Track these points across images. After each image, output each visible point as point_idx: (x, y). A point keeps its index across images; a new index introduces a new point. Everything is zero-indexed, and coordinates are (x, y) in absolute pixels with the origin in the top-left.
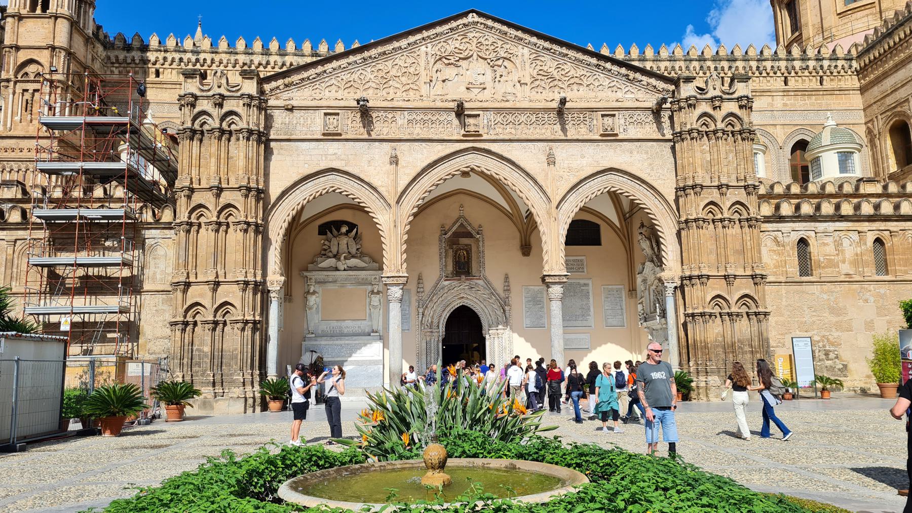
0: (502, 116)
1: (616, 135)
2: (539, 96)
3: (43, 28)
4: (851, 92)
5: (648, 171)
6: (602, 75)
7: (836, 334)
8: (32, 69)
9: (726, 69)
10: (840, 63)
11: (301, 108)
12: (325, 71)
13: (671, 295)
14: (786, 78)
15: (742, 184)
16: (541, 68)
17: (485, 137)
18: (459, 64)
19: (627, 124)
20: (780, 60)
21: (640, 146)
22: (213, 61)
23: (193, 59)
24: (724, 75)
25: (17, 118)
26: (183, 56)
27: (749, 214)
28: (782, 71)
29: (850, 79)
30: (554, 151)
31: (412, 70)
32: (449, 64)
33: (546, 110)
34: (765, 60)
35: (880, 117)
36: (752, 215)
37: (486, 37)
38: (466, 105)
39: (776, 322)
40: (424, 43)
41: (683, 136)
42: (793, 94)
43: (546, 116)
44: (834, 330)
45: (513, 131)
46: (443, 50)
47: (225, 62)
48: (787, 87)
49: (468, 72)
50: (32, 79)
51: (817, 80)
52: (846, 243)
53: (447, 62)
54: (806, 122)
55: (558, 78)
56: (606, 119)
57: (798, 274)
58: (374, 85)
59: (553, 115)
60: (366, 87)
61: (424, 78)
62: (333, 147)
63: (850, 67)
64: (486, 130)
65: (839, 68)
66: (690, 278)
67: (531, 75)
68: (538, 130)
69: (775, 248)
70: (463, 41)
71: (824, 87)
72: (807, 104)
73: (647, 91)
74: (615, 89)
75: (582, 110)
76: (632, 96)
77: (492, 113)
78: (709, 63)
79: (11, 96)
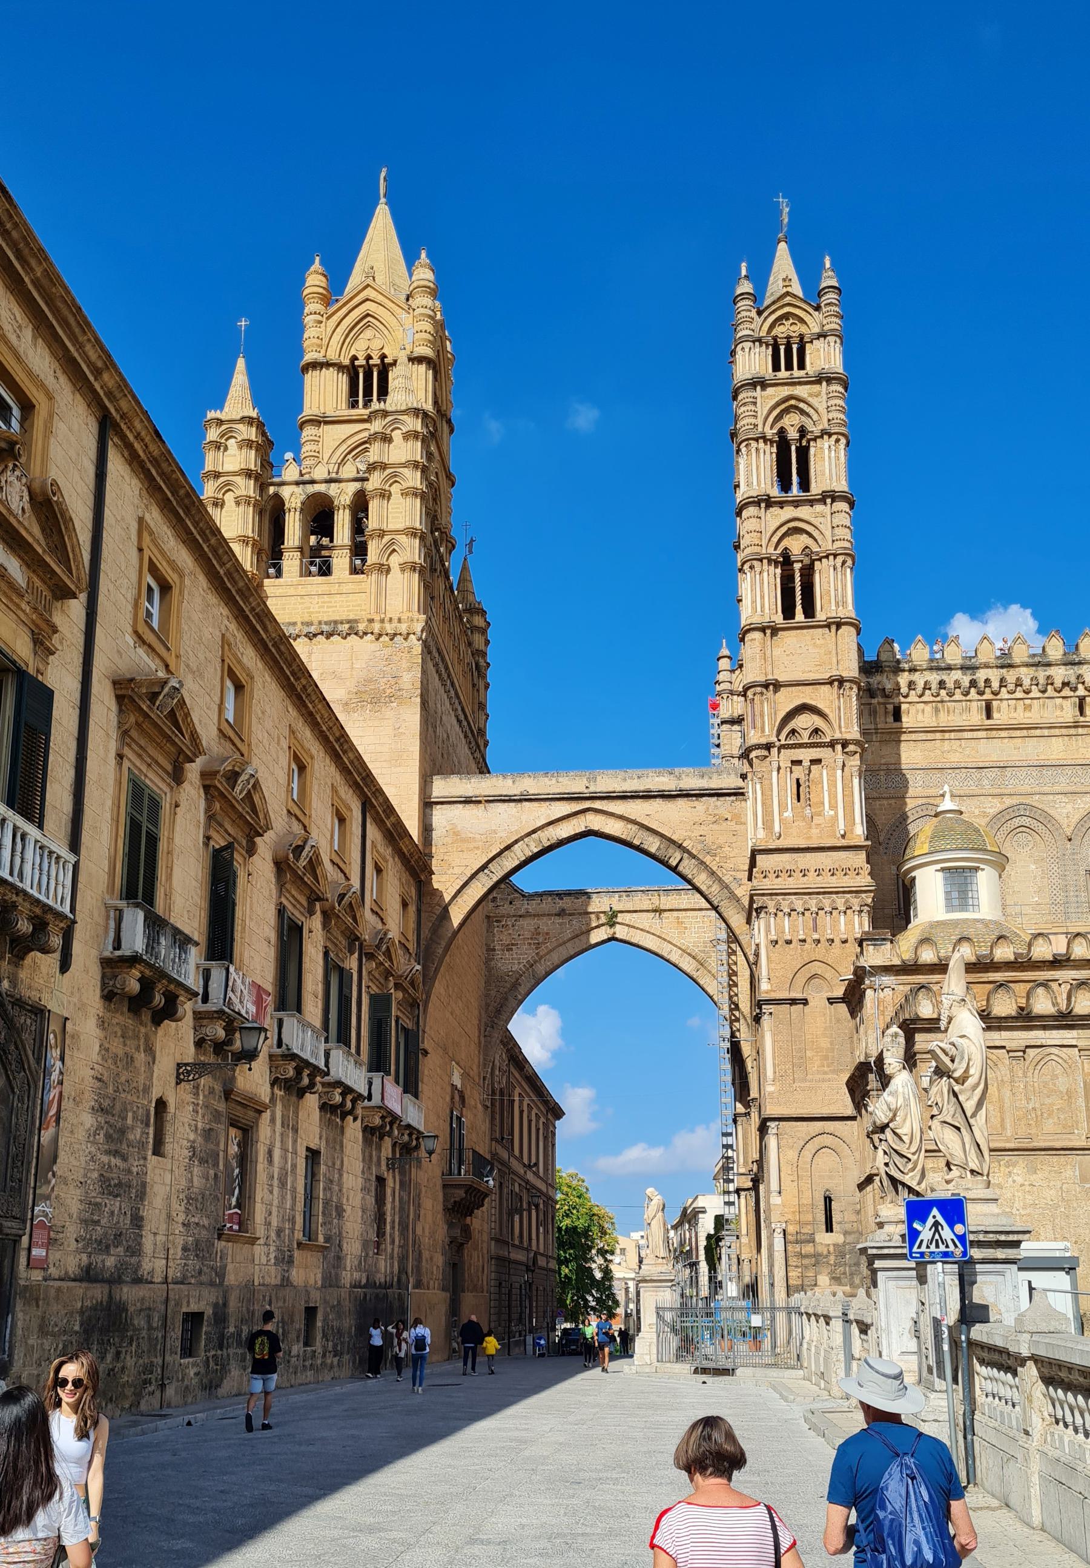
8: (804, 722)
22: (1003, 682)
26: (945, 677)
47: (1026, 682)
50: (806, 741)
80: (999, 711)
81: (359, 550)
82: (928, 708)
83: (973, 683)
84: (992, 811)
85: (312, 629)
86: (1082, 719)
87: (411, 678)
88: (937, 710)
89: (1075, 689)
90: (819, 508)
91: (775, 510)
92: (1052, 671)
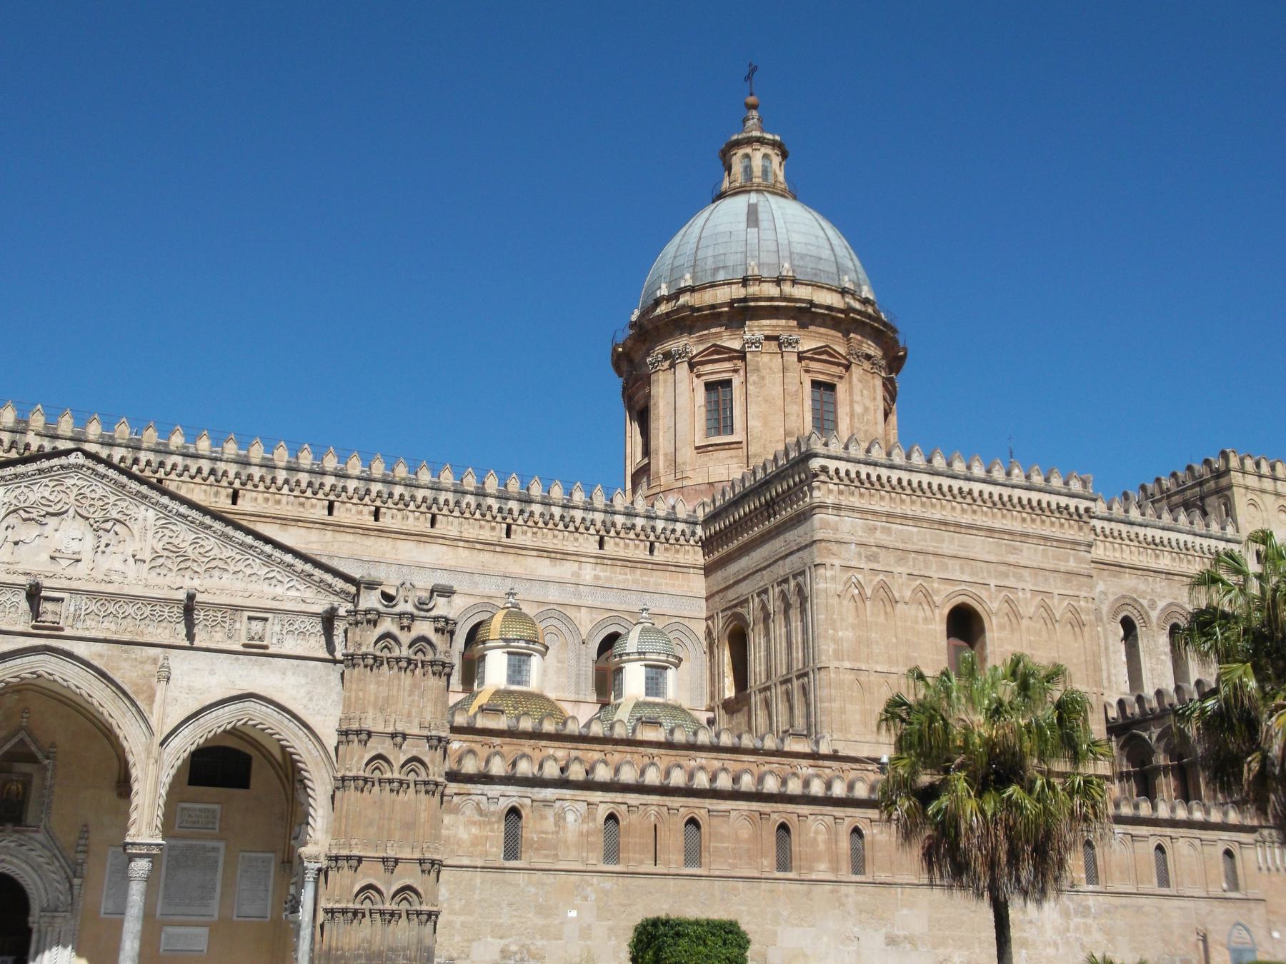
0: (99, 604)
1: (266, 647)
2: (160, 580)
4: (692, 571)
5: (305, 701)
6: (257, 560)
7: (539, 943)
9: (516, 513)
10: (679, 527)
13: (312, 879)
14: (602, 538)
15: (426, 733)
16: (170, 540)
17: (68, 632)
18: (44, 520)
19: (284, 632)
20: (594, 510)
21: (298, 666)
24: (511, 521)
27: (428, 775)
28: (597, 527)
29: (691, 551)
30: (170, 661)
33: (168, 602)
34: (574, 508)
35: (720, 614)
36: (431, 778)
37: (93, 487)
38: (46, 583)
39: (463, 924)
41: (355, 661)
42: (609, 562)
43: (166, 610)
44: (538, 937)
45: (113, 627)
48: (601, 551)
49: (57, 535)
51: (645, 546)
52: (570, 817)
53: (25, 515)
54: (623, 607)
55: (192, 557)
56: (254, 623)
57: (502, 856)
59: (178, 611)
63: (693, 534)
64: (70, 621)
65: (678, 533)
66: (337, 858)
67: (152, 545)
68: (150, 629)
69: (477, 818)
71: (654, 558)
72: (627, 580)
73: (319, 589)
74: (274, 582)
75: (220, 607)
76: (298, 594)
77: (84, 597)
78: (490, 501)
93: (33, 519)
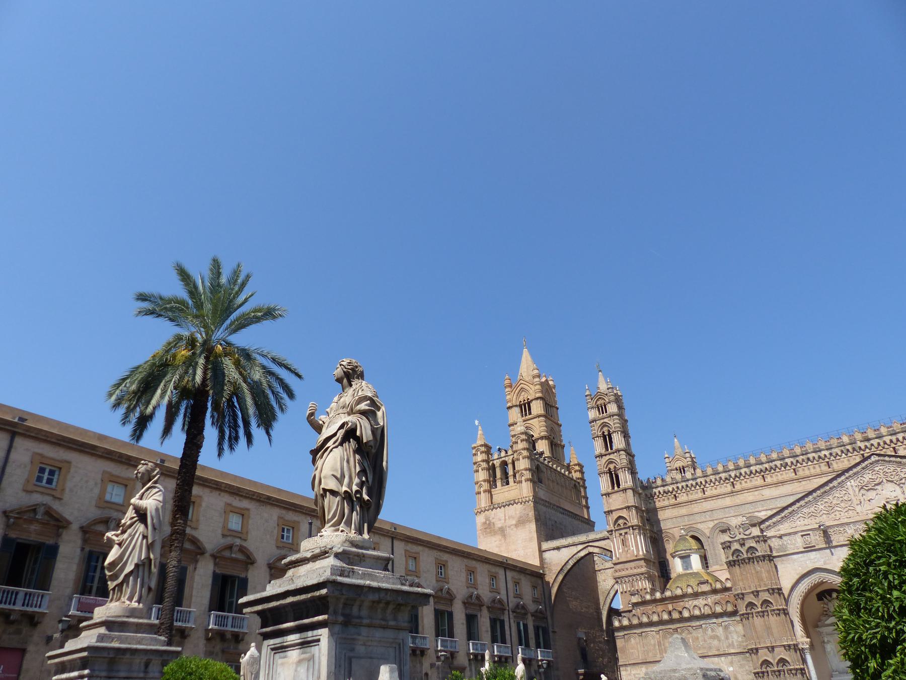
3: (620, 496)
8: (621, 522)
11: (786, 535)
12: (794, 510)
18: (876, 487)
22: (706, 482)
23: (694, 483)
25: (621, 551)
26: (687, 483)
31: (846, 498)
32: (869, 490)
40: (848, 480)
46: (861, 482)
47: (713, 480)
49: (883, 492)
58: (825, 512)
60: (821, 514)
61: (855, 502)
62: (813, 555)
70: (873, 473)
79: (615, 539)
80: (707, 491)
81: (514, 476)
82: (685, 494)
83: (697, 484)
84: (711, 526)
85: (504, 504)
86: (734, 489)
87: (531, 514)
88: (687, 494)
89: (729, 480)
90: (616, 454)
91: (604, 457)
92: (721, 475)
93: (871, 489)
